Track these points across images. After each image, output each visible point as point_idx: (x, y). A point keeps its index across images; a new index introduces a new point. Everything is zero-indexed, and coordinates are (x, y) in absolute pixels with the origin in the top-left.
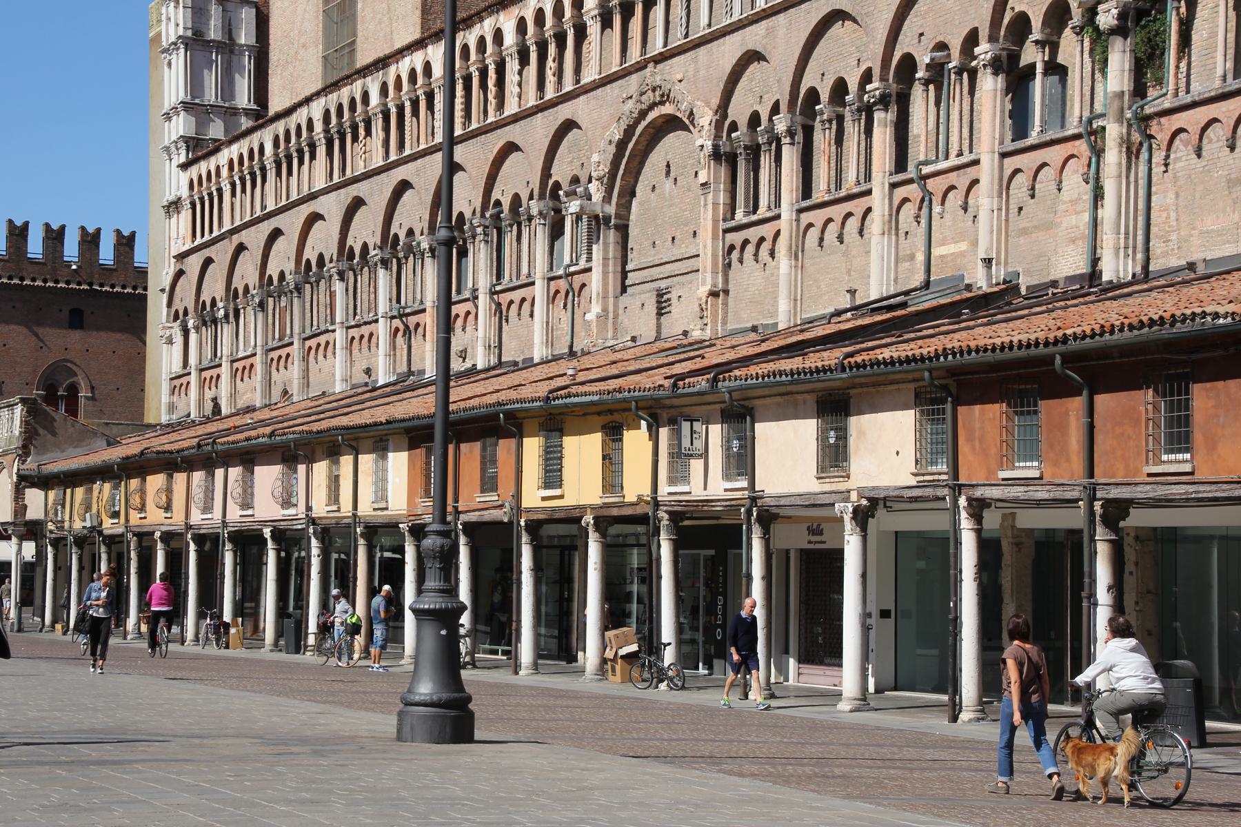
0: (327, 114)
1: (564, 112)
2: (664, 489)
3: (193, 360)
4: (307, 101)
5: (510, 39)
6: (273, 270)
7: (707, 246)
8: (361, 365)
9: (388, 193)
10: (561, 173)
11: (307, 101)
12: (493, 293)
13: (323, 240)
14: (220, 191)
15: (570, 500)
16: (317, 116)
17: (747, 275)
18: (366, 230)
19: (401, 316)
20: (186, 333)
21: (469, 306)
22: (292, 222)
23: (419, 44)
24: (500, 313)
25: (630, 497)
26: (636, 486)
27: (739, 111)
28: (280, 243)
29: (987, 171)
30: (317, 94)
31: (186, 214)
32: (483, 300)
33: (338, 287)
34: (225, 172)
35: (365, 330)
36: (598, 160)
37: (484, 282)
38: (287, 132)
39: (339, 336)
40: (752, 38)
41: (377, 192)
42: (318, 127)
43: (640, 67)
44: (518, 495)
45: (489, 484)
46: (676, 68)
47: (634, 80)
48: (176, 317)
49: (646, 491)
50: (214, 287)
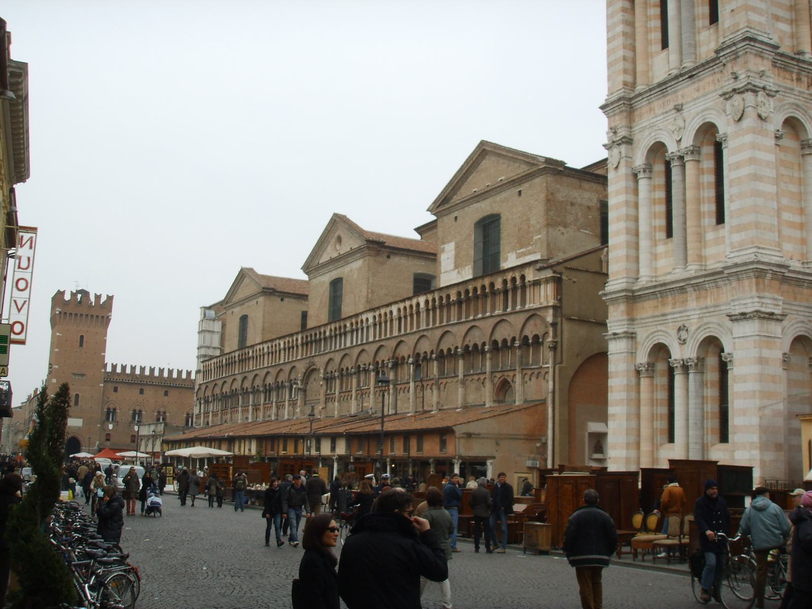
0: (239, 355)
1: (293, 364)
2: (305, 453)
3: (202, 411)
4: (234, 351)
5: (282, 346)
6: (224, 391)
7: (322, 398)
8: (245, 416)
9: (253, 377)
10: (292, 377)
11: (234, 351)
12: (276, 402)
13: (237, 385)
14: (211, 370)
15: (288, 454)
16: (237, 355)
17: (330, 405)
18: (247, 384)
19: (255, 405)
20: (200, 404)
21: (270, 405)
22: (230, 380)
23: (260, 344)
24: (278, 408)
25: (299, 454)
26: (300, 452)
27: (329, 370)
28: (226, 385)
29: (372, 389)
30: (237, 350)
31: (202, 374)
32: (274, 404)
33: (240, 397)
34: (213, 365)
35: (246, 408)
36: (300, 376)
37: (274, 400)
38: (229, 358)
39: (240, 409)
40: (331, 355)
41: (251, 376)
42: (237, 359)
43: (309, 357)
44: (278, 453)
45: (272, 450)
46: (316, 359)
47: (308, 361)
48: (198, 399)
49: (302, 453)
50: (209, 393)
